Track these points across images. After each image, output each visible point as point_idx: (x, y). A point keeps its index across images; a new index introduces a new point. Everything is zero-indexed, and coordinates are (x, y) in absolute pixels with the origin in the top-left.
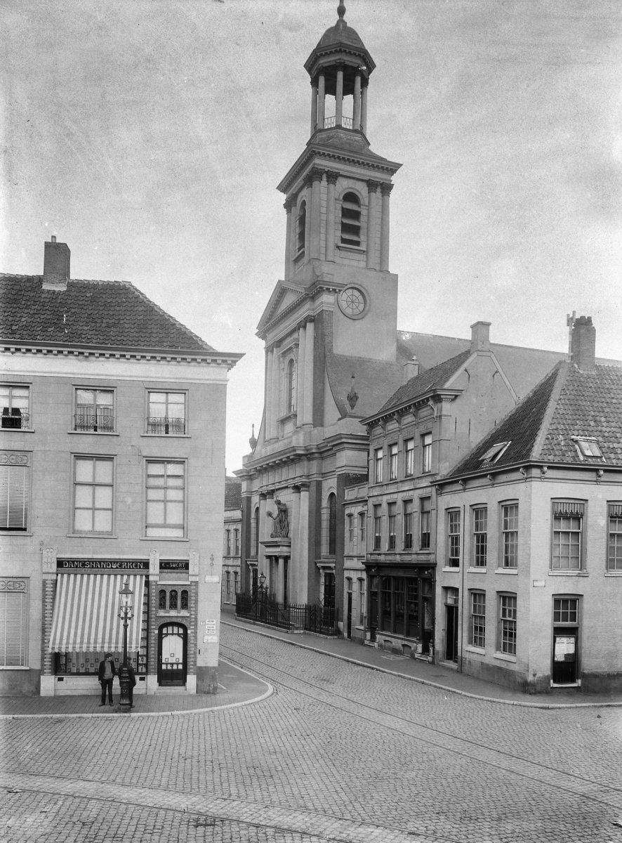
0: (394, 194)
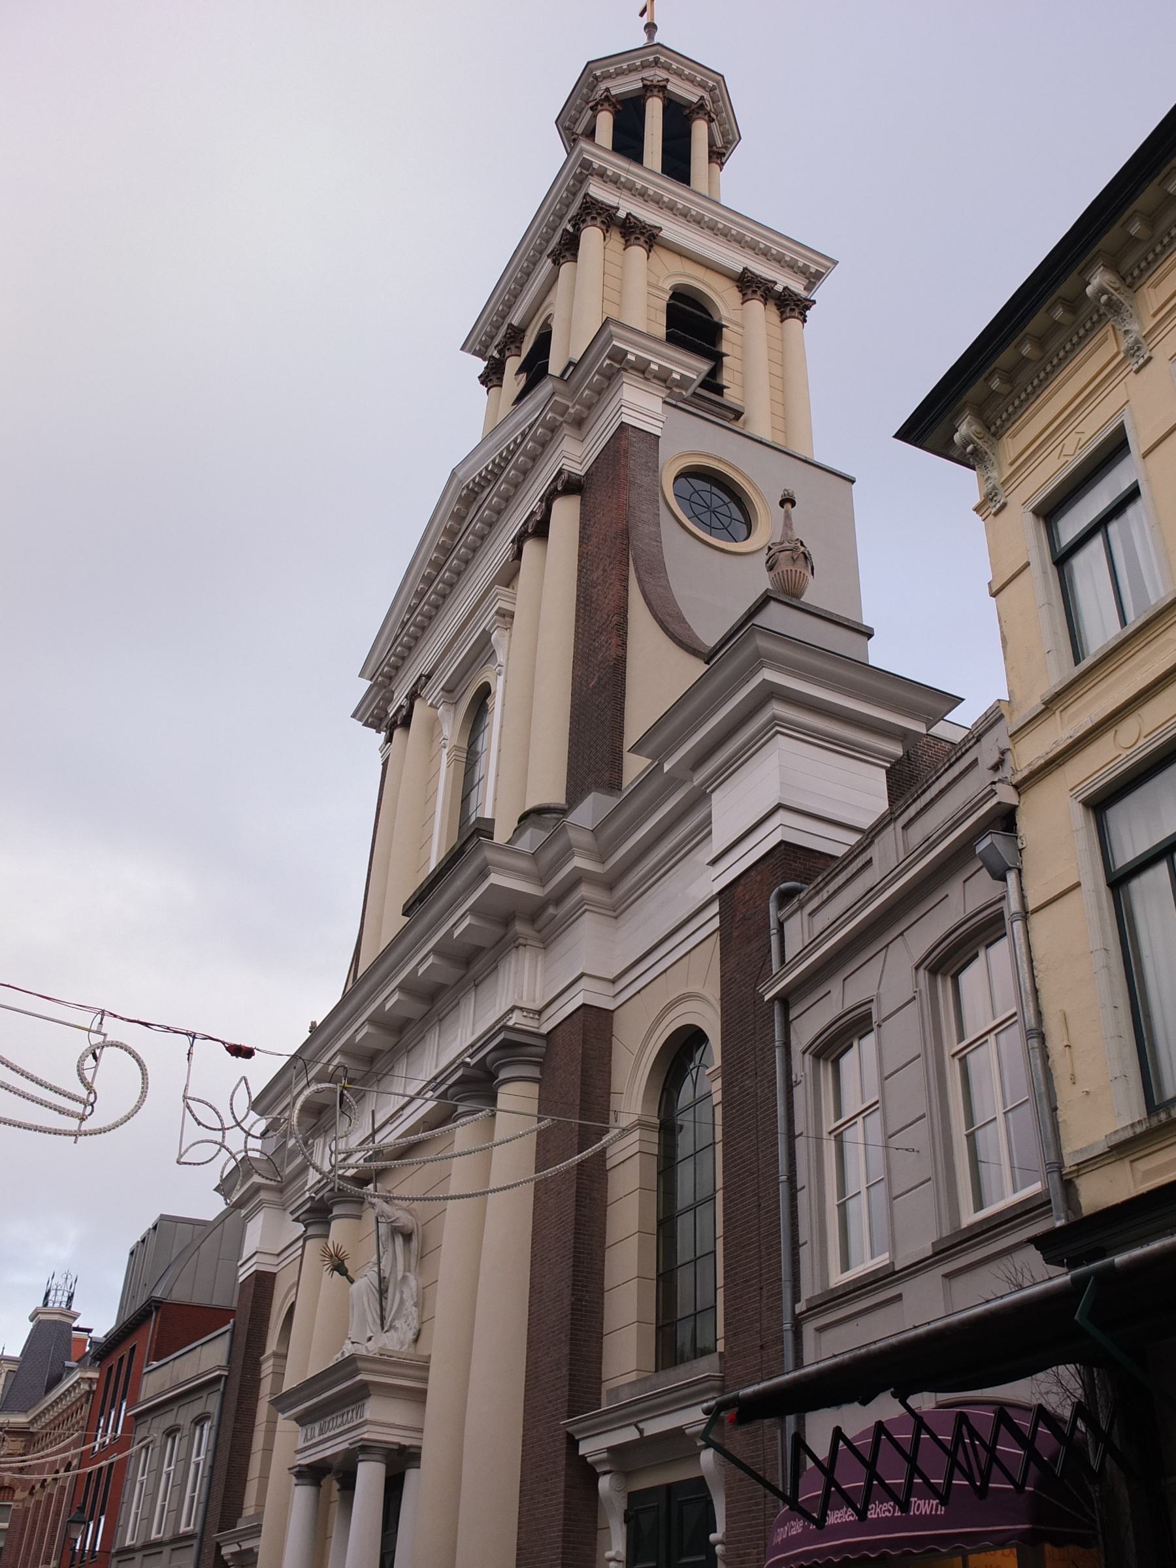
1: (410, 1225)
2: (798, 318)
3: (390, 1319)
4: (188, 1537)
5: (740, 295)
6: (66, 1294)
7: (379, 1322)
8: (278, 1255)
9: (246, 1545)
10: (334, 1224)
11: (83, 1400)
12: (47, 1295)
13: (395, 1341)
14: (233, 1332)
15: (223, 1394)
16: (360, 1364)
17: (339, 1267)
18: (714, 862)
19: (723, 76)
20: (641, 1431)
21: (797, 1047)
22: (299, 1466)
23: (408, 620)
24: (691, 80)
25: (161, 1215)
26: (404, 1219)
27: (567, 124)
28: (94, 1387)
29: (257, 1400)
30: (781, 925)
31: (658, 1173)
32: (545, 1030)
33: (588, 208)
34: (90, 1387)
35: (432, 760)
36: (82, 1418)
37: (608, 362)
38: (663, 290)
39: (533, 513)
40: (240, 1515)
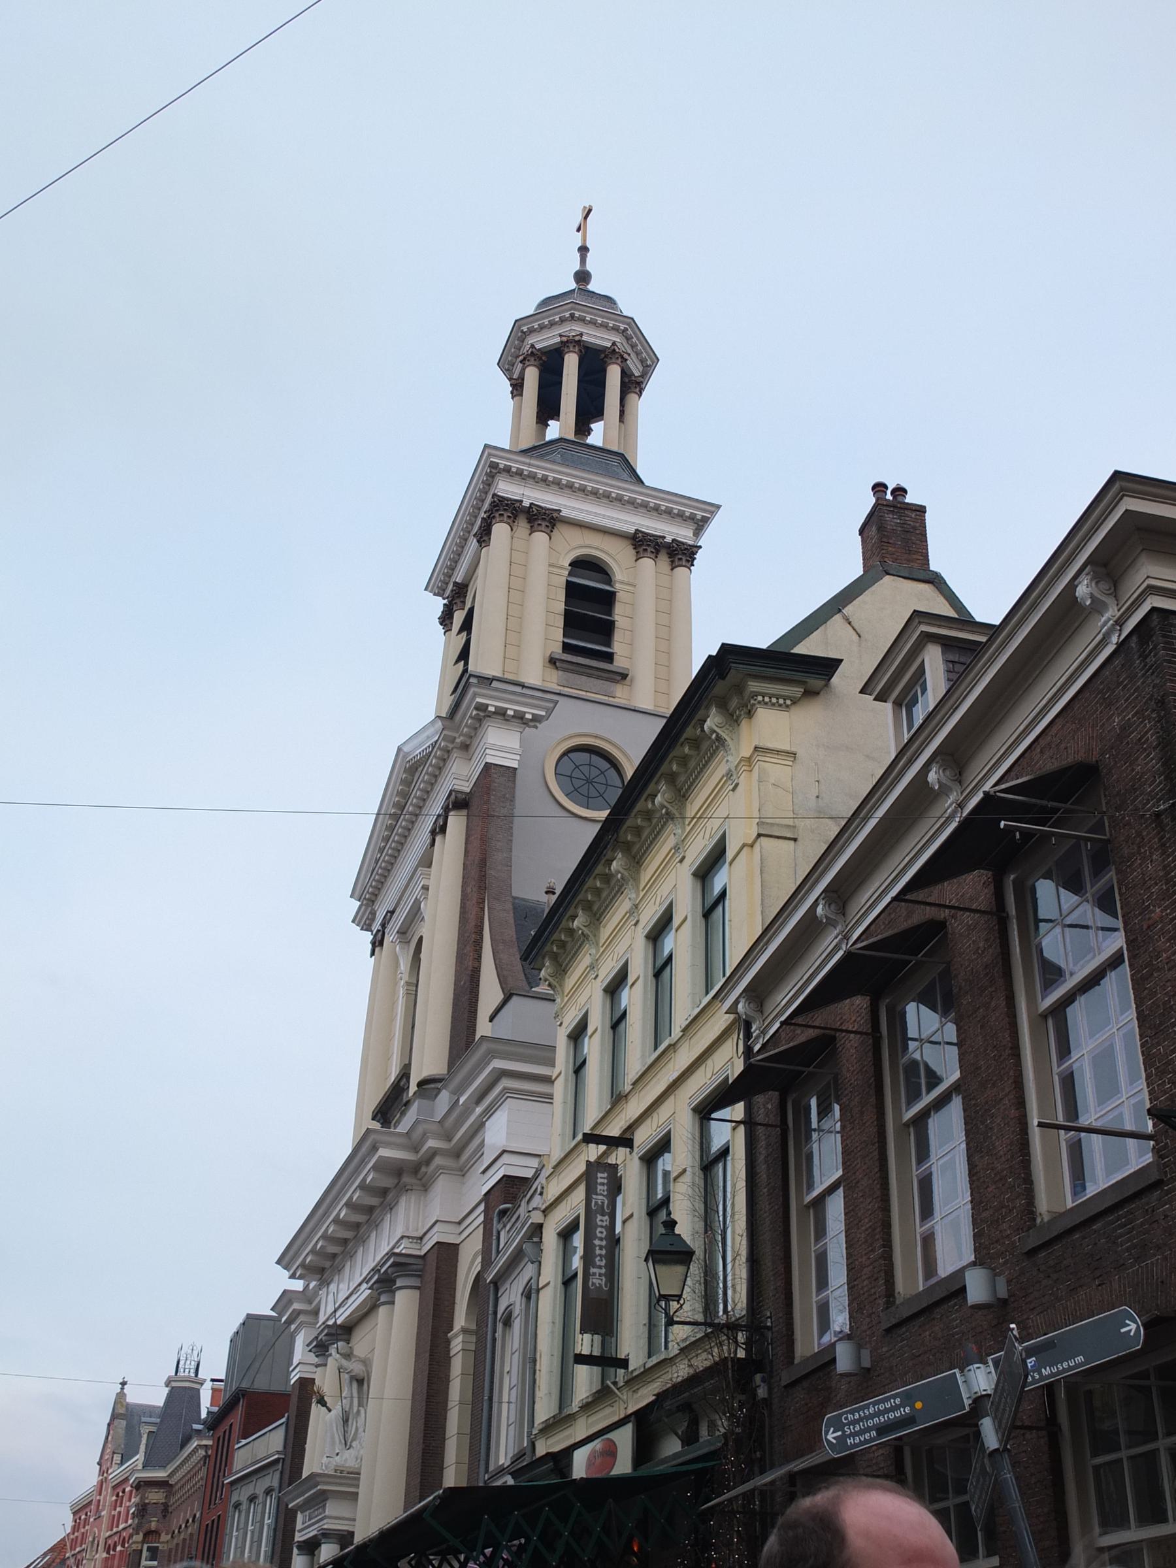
1: (361, 1374)
2: (685, 566)
5: (634, 552)
7: (343, 1442)
11: (202, 1463)
14: (287, 1423)
16: (319, 1479)
18: (484, 1172)
19: (632, 319)
24: (604, 326)
25: (248, 1315)
26: (356, 1368)
27: (507, 367)
28: (210, 1452)
32: (422, 1253)
33: (497, 506)
34: (206, 1452)
36: (202, 1478)
37: (475, 712)
38: (564, 568)
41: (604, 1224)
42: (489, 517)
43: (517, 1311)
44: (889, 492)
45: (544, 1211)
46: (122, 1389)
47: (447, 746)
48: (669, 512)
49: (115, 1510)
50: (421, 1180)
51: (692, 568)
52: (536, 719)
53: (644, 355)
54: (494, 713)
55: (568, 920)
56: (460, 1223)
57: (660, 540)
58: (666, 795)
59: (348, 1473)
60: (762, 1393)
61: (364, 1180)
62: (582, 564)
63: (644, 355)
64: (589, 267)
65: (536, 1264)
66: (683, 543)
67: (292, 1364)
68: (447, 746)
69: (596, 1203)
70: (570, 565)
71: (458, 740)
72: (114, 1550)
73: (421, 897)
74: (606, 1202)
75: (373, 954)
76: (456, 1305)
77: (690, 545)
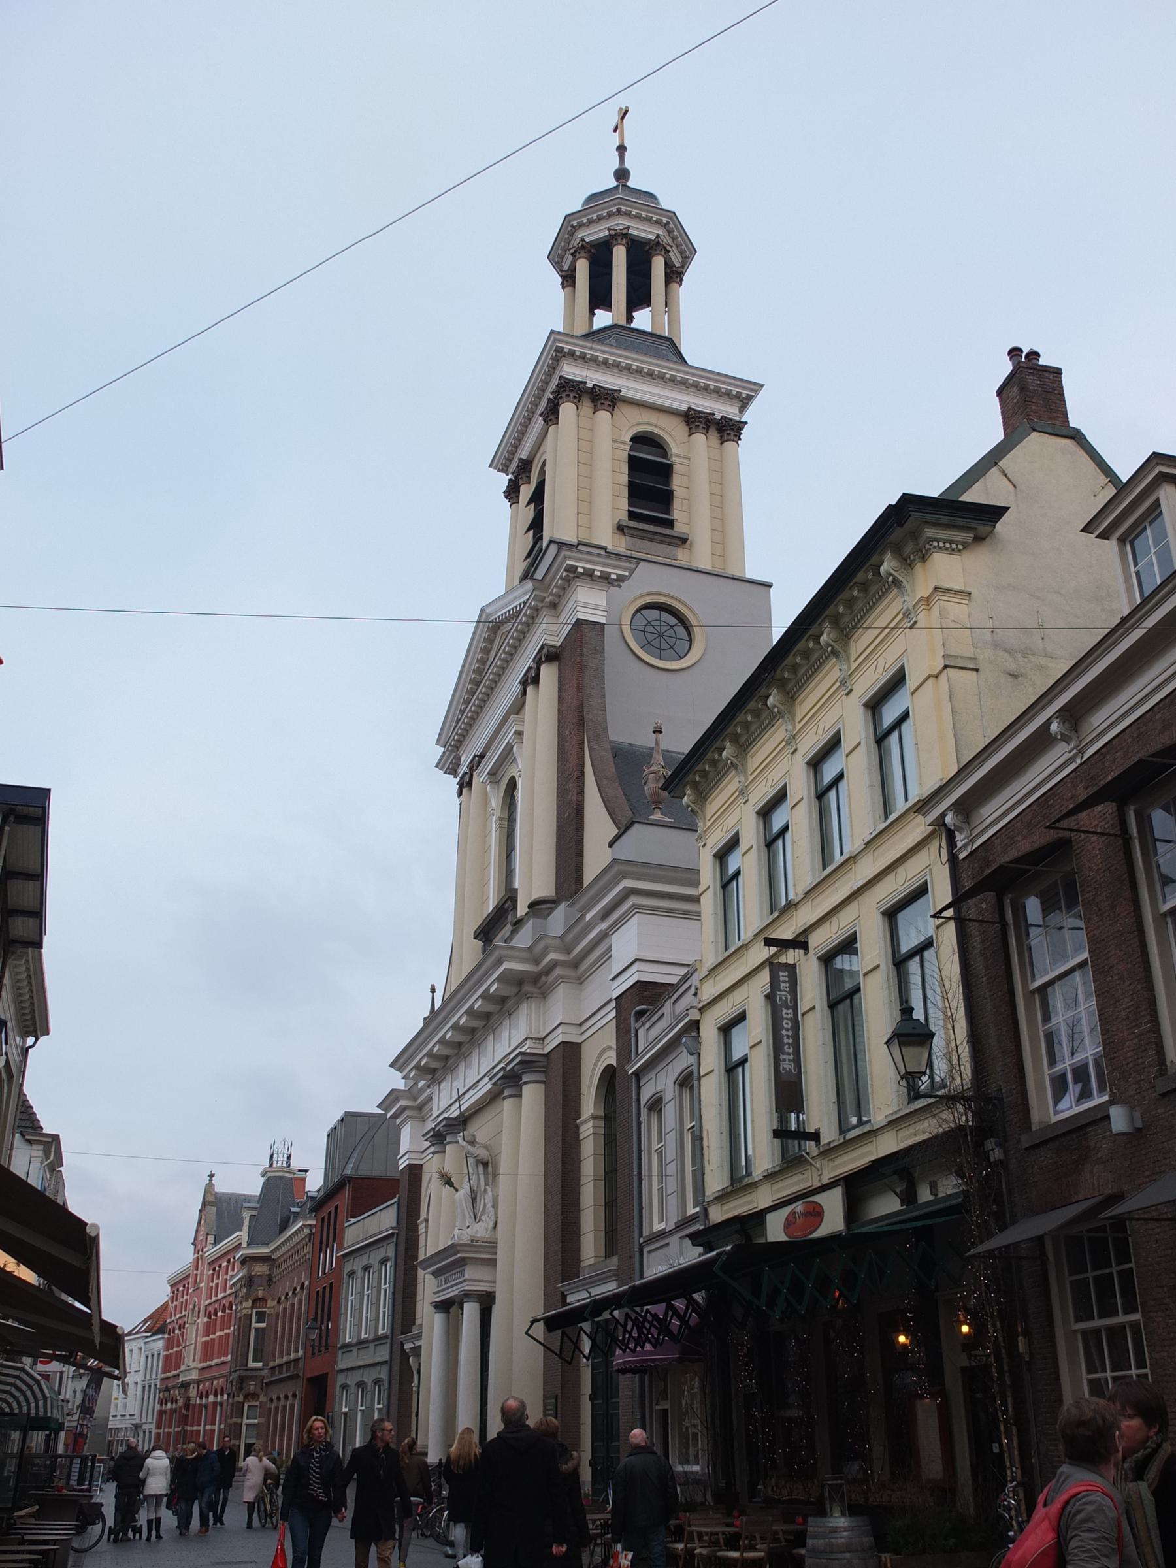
0: (748, 445)
1: (486, 1158)
2: (733, 441)
3: (479, 1215)
4: (384, 1337)
5: (687, 428)
6: (285, 1156)
7: (473, 1216)
8: (423, 1152)
9: (417, 1344)
10: (448, 1147)
11: (307, 1240)
12: (272, 1157)
13: (481, 1230)
15: (396, 1245)
16: (459, 1248)
17: (449, 1183)
18: (613, 979)
19: (674, 213)
20: (589, 1293)
21: (643, 1103)
22: (436, 1302)
23: (466, 709)
24: (648, 220)
26: (482, 1153)
27: (556, 260)
28: (314, 1231)
29: (418, 1249)
30: (637, 1031)
31: (605, 1145)
32: (546, 1051)
33: (564, 387)
35: (486, 820)
36: (308, 1253)
37: (565, 574)
38: (625, 443)
39: (530, 668)
40: (414, 1324)
41: (789, 1016)
42: (555, 398)
43: (668, 1096)
44: (1024, 355)
45: (700, 1010)
46: (211, 1180)
47: (537, 605)
48: (717, 391)
49: (212, 1282)
50: (540, 988)
51: (739, 442)
52: (621, 579)
53: (684, 247)
54: (583, 574)
55: (713, 752)
56: (581, 1025)
57: (710, 417)
58: (831, 635)
59: (483, 1242)
60: (997, 1154)
61: (488, 990)
62: (642, 440)
63: (684, 247)
64: (627, 165)
65: (696, 1056)
66: (731, 420)
67: (399, 1154)
68: (537, 605)
69: (780, 998)
70: (631, 440)
71: (547, 600)
72: (216, 1315)
73: (513, 741)
74: (789, 997)
75: (460, 794)
76: (582, 1096)
77: (737, 421)
